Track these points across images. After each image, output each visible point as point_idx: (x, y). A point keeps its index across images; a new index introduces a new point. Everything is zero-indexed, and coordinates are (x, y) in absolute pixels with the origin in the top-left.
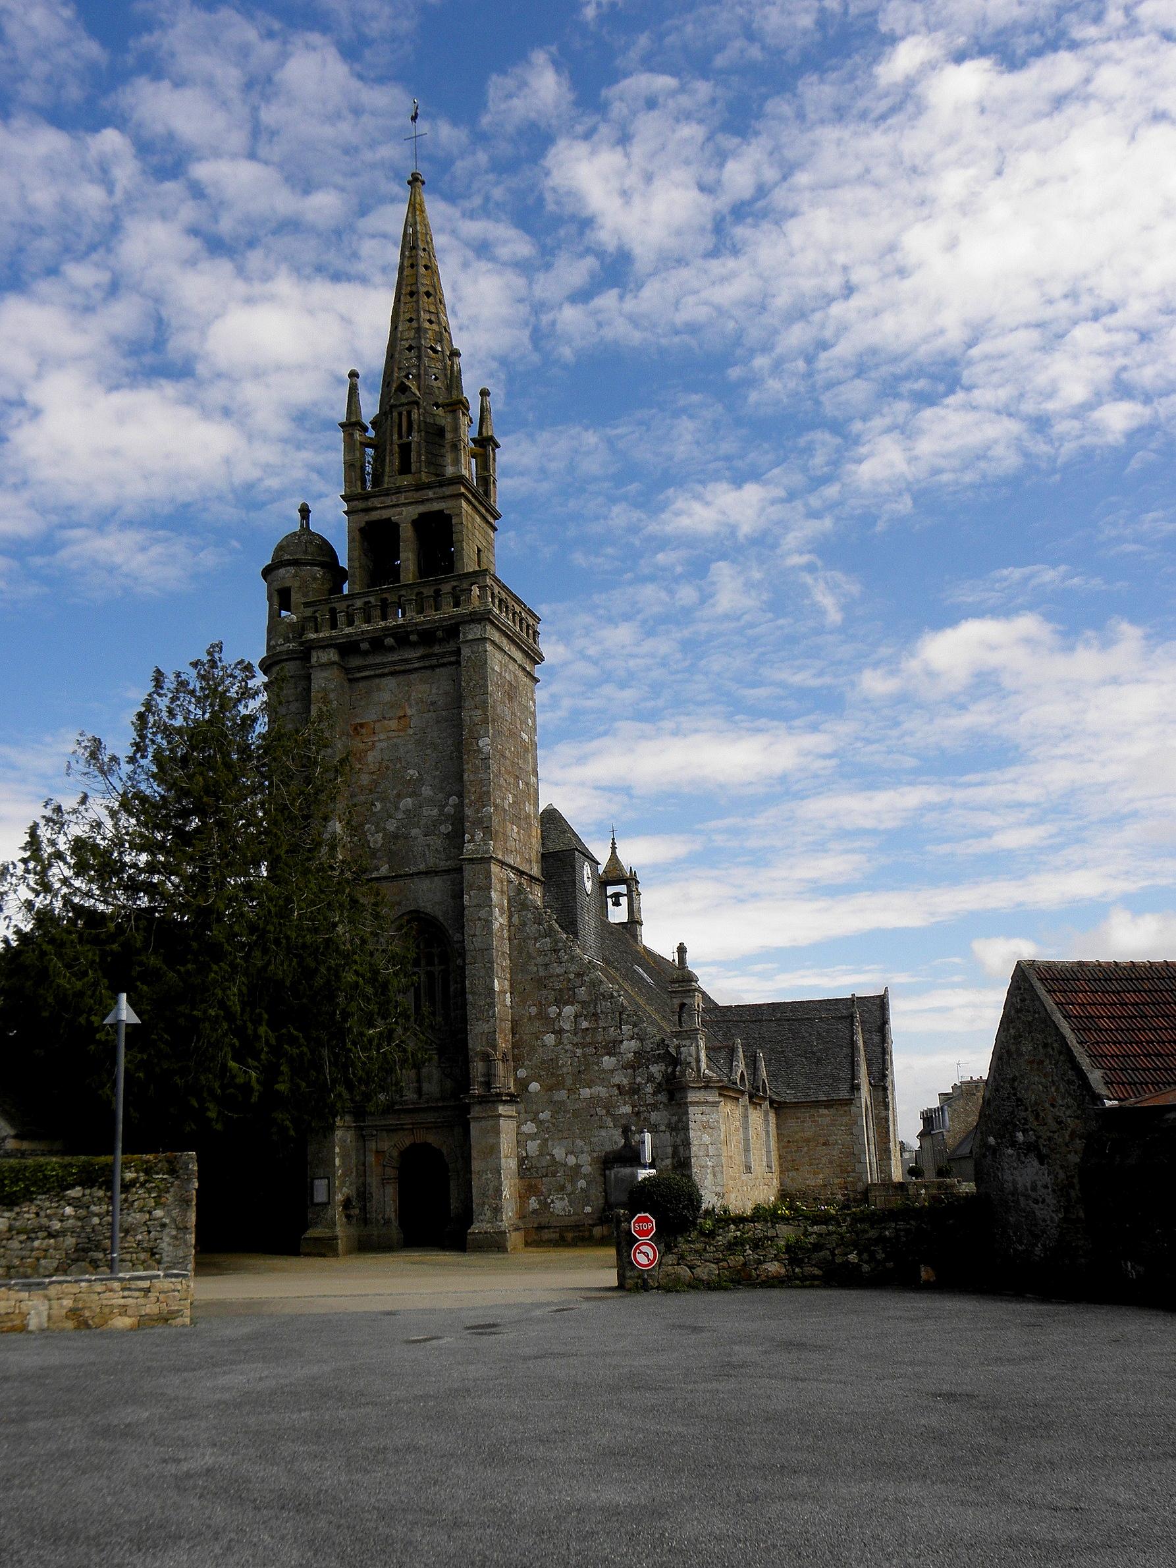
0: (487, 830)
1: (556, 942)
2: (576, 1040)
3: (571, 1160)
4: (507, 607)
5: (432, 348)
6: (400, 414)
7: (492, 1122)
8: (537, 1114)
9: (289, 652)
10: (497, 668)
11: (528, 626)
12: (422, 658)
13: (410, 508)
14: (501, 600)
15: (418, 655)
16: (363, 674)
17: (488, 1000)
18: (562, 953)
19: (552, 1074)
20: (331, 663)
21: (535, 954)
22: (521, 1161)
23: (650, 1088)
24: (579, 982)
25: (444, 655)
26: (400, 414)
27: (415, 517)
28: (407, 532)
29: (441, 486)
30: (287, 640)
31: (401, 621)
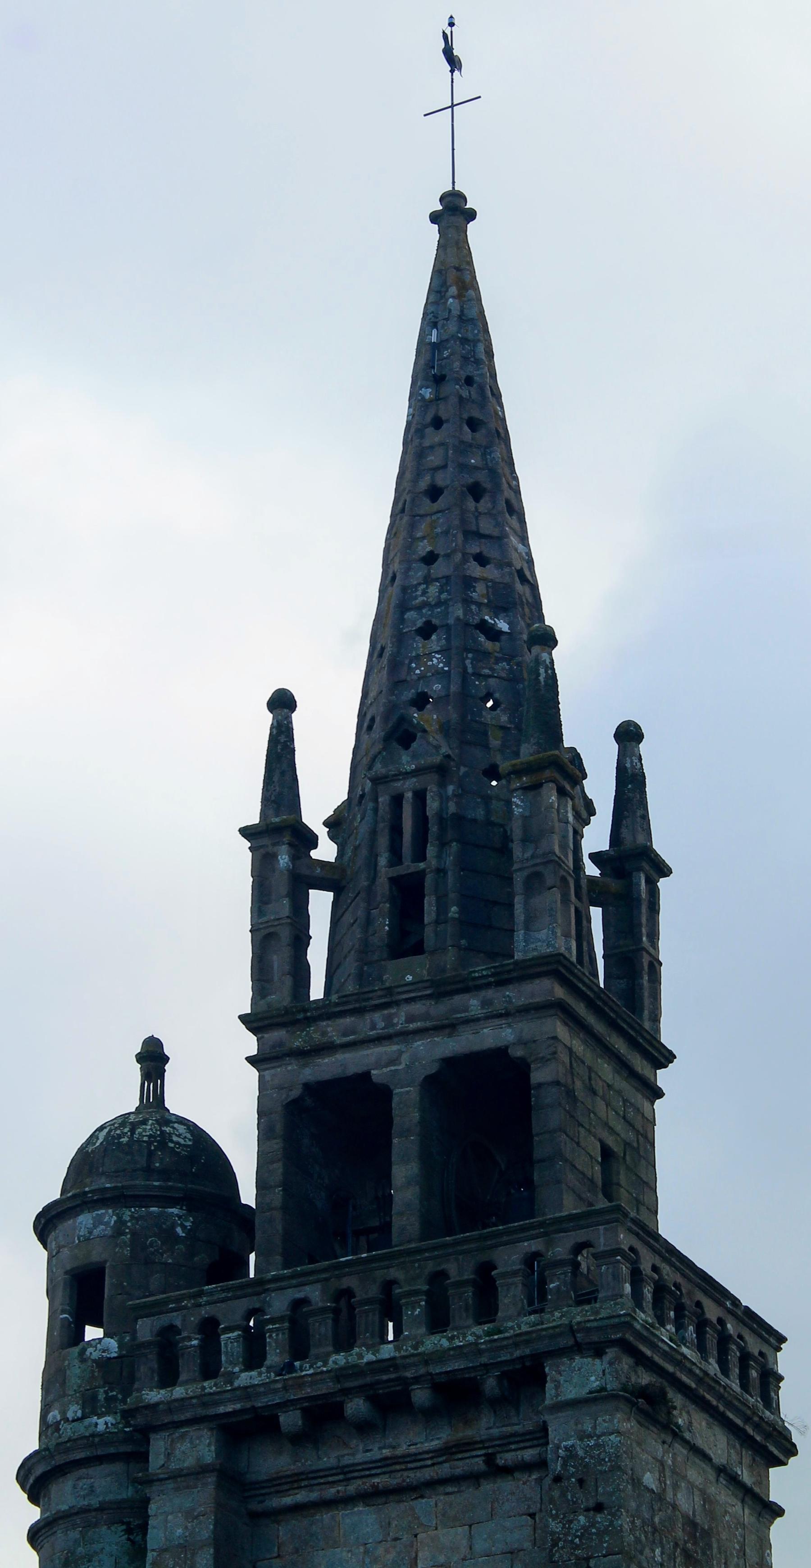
4: (680, 1309)
6: (397, 800)
9: (93, 1439)
10: (649, 1479)
11: (745, 1358)
12: (449, 1451)
13: (420, 1045)
14: (660, 1290)
15: (435, 1444)
16: (288, 1500)
20: (201, 1471)
25: (507, 1441)
26: (397, 800)
27: (433, 1069)
28: (407, 1107)
29: (502, 983)
30: (90, 1406)
31: (387, 1352)
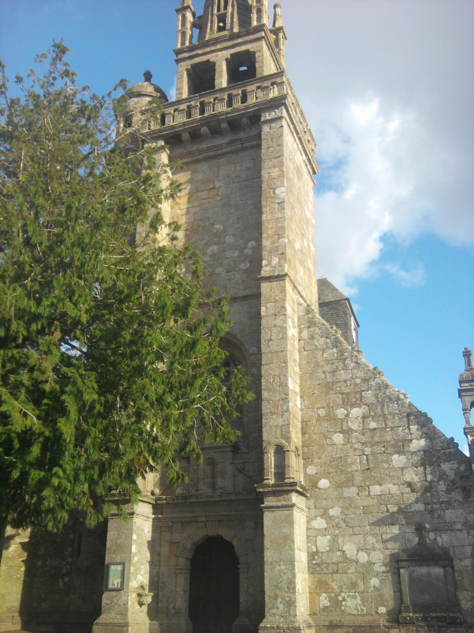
0: (283, 255)
1: (342, 352)
2: (364, 439)
3: (363, 557)
7: (286, 513)
8: (326, 510)
12: (230, 143)
13: (224, 52)
17: (283, 396)
18: (348, 361)
19: (342, 471)
21: (323, 363)
22: (312, 556)
23: (442, 486)
24: (365, 387)
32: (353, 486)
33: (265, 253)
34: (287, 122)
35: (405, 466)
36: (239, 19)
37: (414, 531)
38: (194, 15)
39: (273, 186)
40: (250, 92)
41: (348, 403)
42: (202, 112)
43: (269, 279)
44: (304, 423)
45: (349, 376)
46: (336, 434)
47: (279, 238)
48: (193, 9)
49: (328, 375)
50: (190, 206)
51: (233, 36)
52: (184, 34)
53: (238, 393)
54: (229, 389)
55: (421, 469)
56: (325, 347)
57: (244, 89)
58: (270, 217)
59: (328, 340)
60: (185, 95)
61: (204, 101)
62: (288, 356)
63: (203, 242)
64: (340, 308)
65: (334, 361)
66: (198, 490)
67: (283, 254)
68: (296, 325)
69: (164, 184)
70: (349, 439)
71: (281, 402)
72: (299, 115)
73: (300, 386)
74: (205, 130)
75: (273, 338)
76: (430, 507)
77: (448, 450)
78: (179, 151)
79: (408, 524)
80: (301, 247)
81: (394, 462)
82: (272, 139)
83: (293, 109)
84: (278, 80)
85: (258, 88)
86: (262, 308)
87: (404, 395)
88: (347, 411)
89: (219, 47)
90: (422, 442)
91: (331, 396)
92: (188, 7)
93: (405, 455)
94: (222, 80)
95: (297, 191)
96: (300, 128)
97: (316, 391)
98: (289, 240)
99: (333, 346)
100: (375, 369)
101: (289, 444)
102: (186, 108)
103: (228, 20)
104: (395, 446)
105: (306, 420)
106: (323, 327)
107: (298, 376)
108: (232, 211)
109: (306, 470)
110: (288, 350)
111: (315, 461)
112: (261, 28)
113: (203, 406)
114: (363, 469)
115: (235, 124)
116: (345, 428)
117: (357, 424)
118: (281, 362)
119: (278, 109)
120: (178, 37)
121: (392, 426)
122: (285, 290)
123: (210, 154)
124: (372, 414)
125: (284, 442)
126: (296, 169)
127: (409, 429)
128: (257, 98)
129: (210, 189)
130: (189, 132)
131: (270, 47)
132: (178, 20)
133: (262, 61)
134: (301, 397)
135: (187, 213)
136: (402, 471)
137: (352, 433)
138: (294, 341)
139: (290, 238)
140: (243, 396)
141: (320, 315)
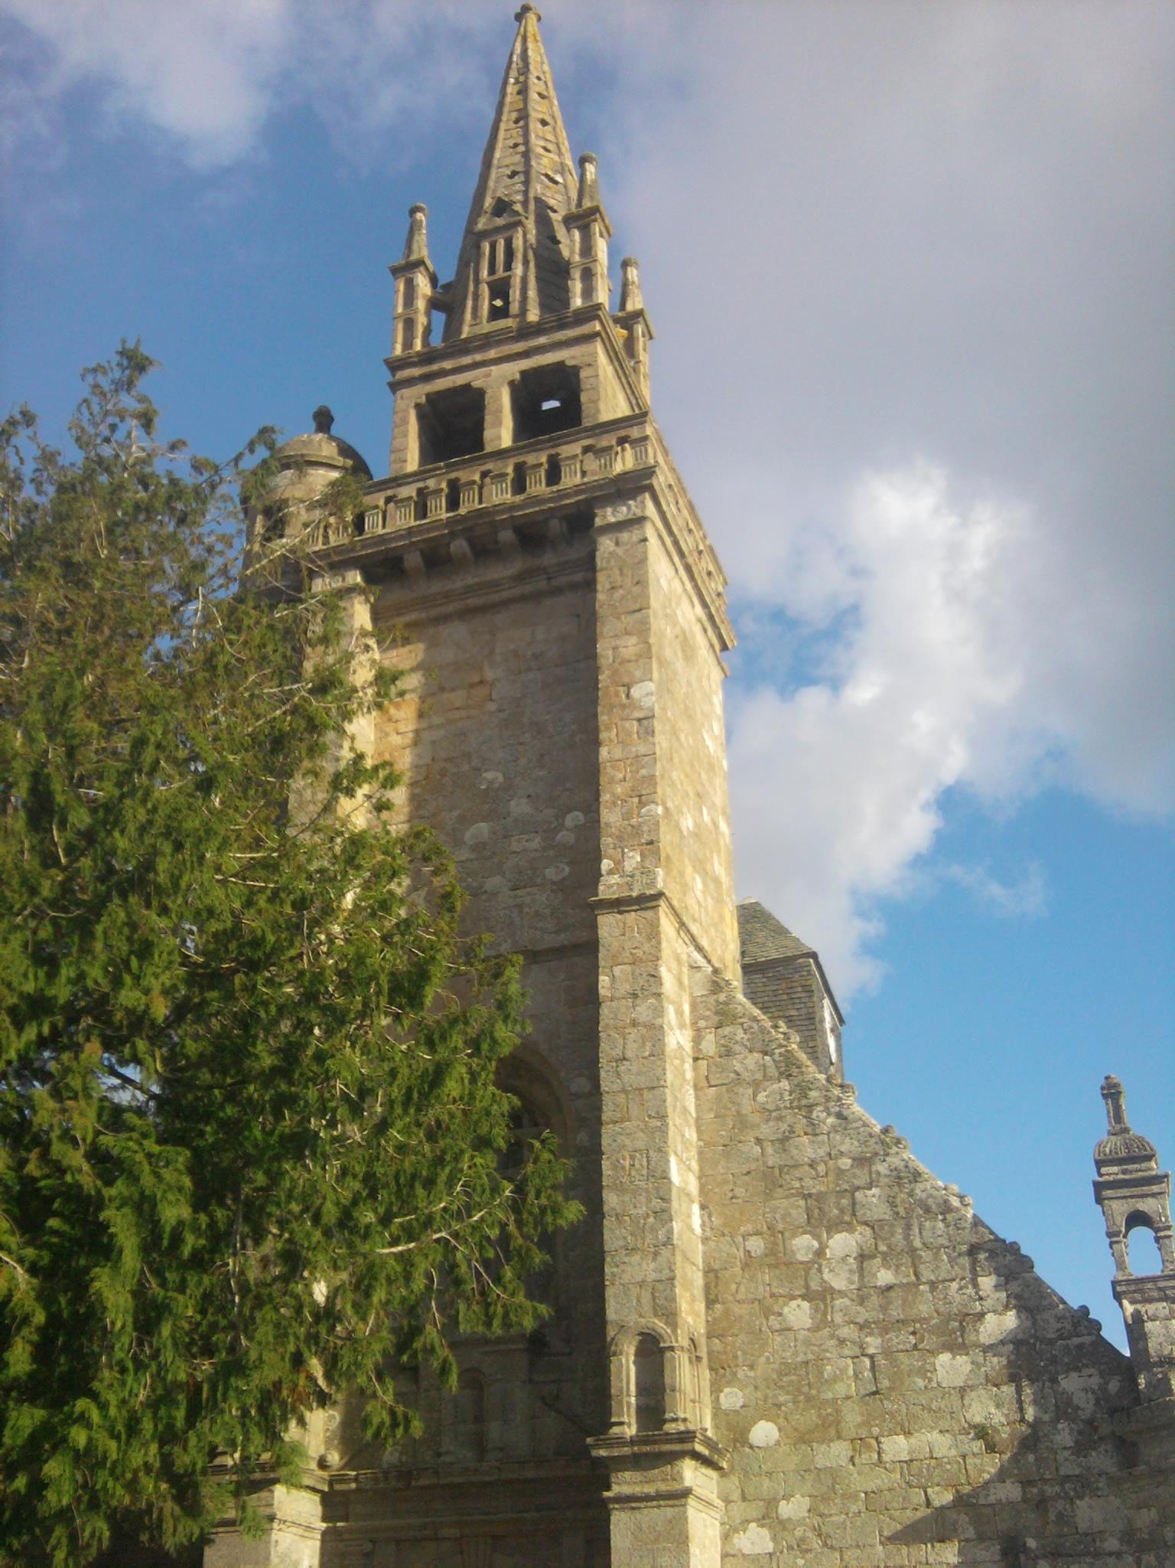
1: (802, 1089)
2: (863, 1315)
5: (547, 176)
7: (669, 1512)
8: (771, 1503)
12: (521, 578)
17: (656, 1203)
18: (818, 1113)
19: (809, 1399)
21: (755, 1118)
23: (1064, 1435)
24: (862, 1179)
32: (839, 1438)
33: (607, 842)
34: (657, 530)
35: (970, 1383)
36: (541, 292)
37: (997, 1557)
38: (434, 280)
39: (626, 680)
40: (568, 458)
41: (821, 1219)
42: (453, 503)
43: (618, 905)
44: (711, 1275)
45: (822, 1152)
46: (794, 1304)
47: (642, 804)
48: (431, 268)
49: (770, 1150)
50: (424, 725)
51: (527, 331)
52: (409, 324)
53: (544, 1201)
54: (520, 1190)
55: (1008, 1390)
56: (759, 1076)
57: (553, 451)
58: (618, 753)
59: (767, 1058)
60: (412, 464)
61: (457, 480)
62: (669, 1100)
63: (456, 813)
64: (796, 976)
65: (784, 1113)
66: (439, 1455)
67: (651, 843)
68: (688, 1021)
69: (361, 674)
70: (825, 1314)
71: (651, 1220)
72: (685, 512)
73: (700, 1178)
74: (459, 546)
75: (629, 1054)
76: (1035, 1491)
77: (1076, 1341)
78: (399, 595)
79: (981, 1538)
80: (697, 825)
81: (941, 1372)
82: (621, 570)
83: (671, 500)
84: (635, 433)
85: (587, 450)
86: (601, 978)
87: (961, 1198)
88: (820, 1243)
89: (492, 354)
90: (1010, 1320)
91: (776, 1203)
92: (421, 263)
93: (967, 1354)
94: (501, 431)
95: (684, 690)
96: (687, 543)
97: (740, 1191)
98: (666, 809)
99: (781, 1074)
100: (886, 1131)
101: (674, 1331)
102: (414, 494)
103: (515, 294)
104: (941, 1330)
105: (716, 1267)
106: (755, 1025)
107: (694, 1153)
108: (527, 737)
109: (717, 1399)
110: (668, 1084)
111: (740, 1375)
112: (592, 312)
113: (456, 1235)
114: (862, 1392)
115: (531, 534)
116: (814, 1286)
117: (844, 1275)
118: (649, 1116)
119: (634, 498)
120: (395, 330)
121: (933, 1278)
122: (658, 934)
123: (472, 602)
124: (883, 1248)
125: (660, 1325)
126: (681, 638)
127: (976, 1285)
128: (584, 473)
129: (472, 686)
130: (422, 552)
131: (613, 356)
132: (397, 292)
133: (595, 388)
134: (703, 1207)
135: (416, 743)
136: (962, 1398)
137: (833, 1299)
138: (683, 1061)
139: (669, 804)
140: (556, 1210)
141: (745, 995)
